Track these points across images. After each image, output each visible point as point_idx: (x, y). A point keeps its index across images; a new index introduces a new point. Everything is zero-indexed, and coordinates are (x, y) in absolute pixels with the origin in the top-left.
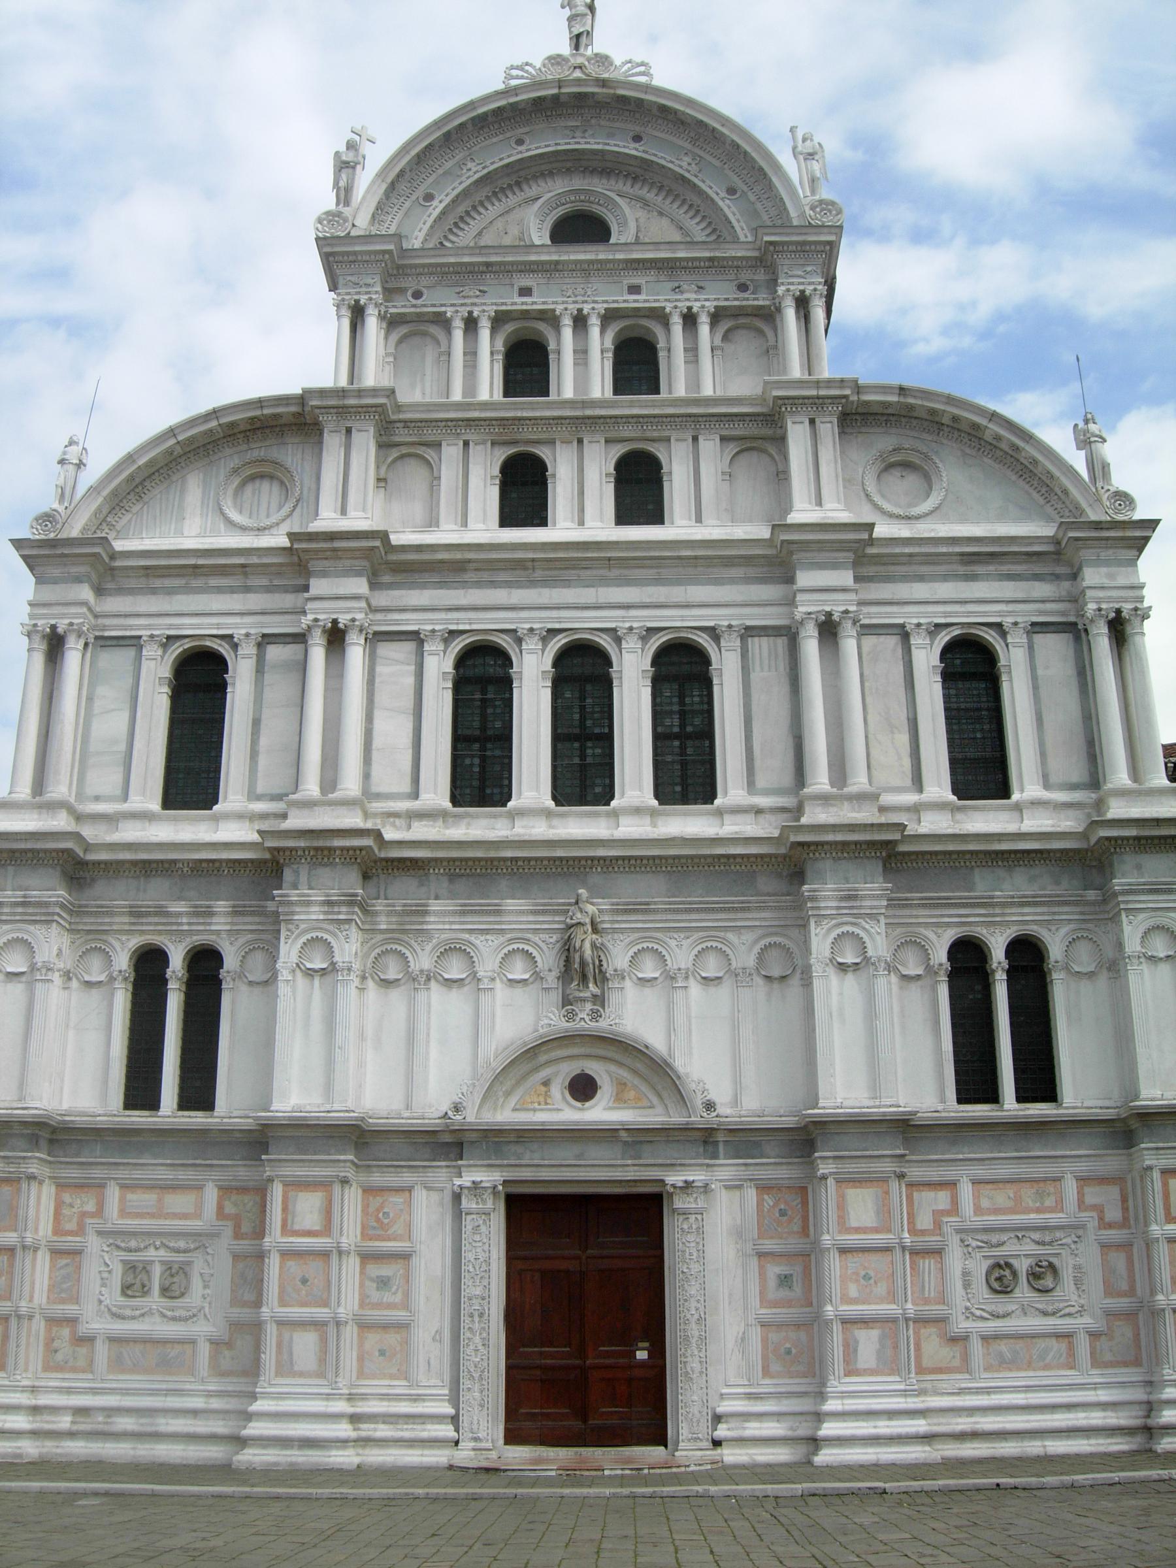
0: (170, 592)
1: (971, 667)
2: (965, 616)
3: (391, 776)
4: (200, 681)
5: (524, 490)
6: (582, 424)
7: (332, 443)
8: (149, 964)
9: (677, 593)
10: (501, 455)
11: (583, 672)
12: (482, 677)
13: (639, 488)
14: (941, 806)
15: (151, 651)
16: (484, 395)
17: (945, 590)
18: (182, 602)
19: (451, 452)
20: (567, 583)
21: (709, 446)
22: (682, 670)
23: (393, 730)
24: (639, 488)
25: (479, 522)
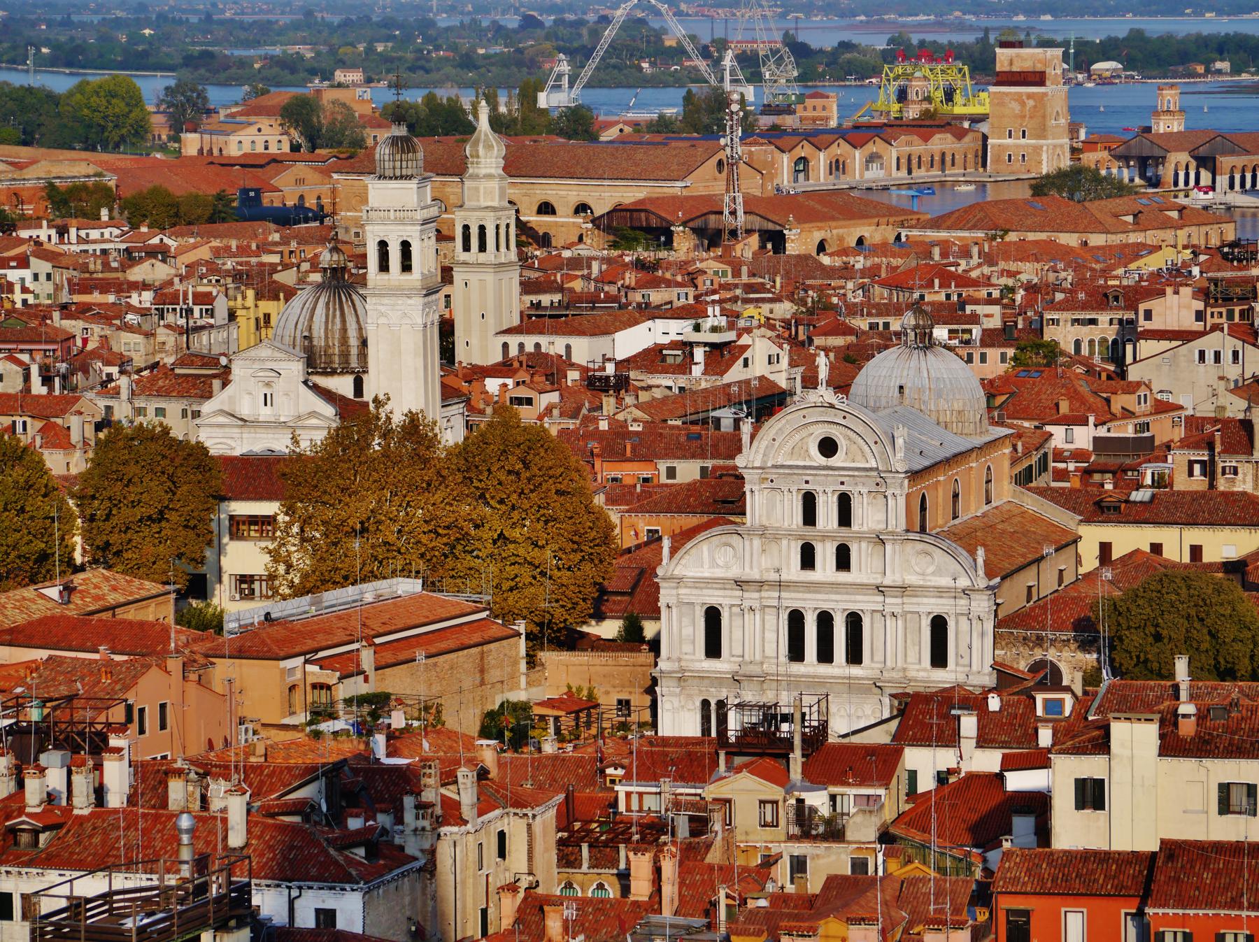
0: (701, 588)
1: (939, 626)
2: (937, 611)
3: (771, 651)
4: (713, 617)
5: (808, 558)
6: (824, 538)
7: (747, 543)
8: (705, 704)
9: (853, 598)
10: (800, 543)
11: (825, 620)
12: (796, 619)
13: (843, 561)
14: (925, 670)
15: (698, 608)
16: (794, 527)
17: (933, 601)
18: (706, 592)
19: (785, 542)
20: (819, 592)
21: (864, 545)
22: (854, 622)
23: (770, 636)
24: (843, 561)
25: (792, 569)
